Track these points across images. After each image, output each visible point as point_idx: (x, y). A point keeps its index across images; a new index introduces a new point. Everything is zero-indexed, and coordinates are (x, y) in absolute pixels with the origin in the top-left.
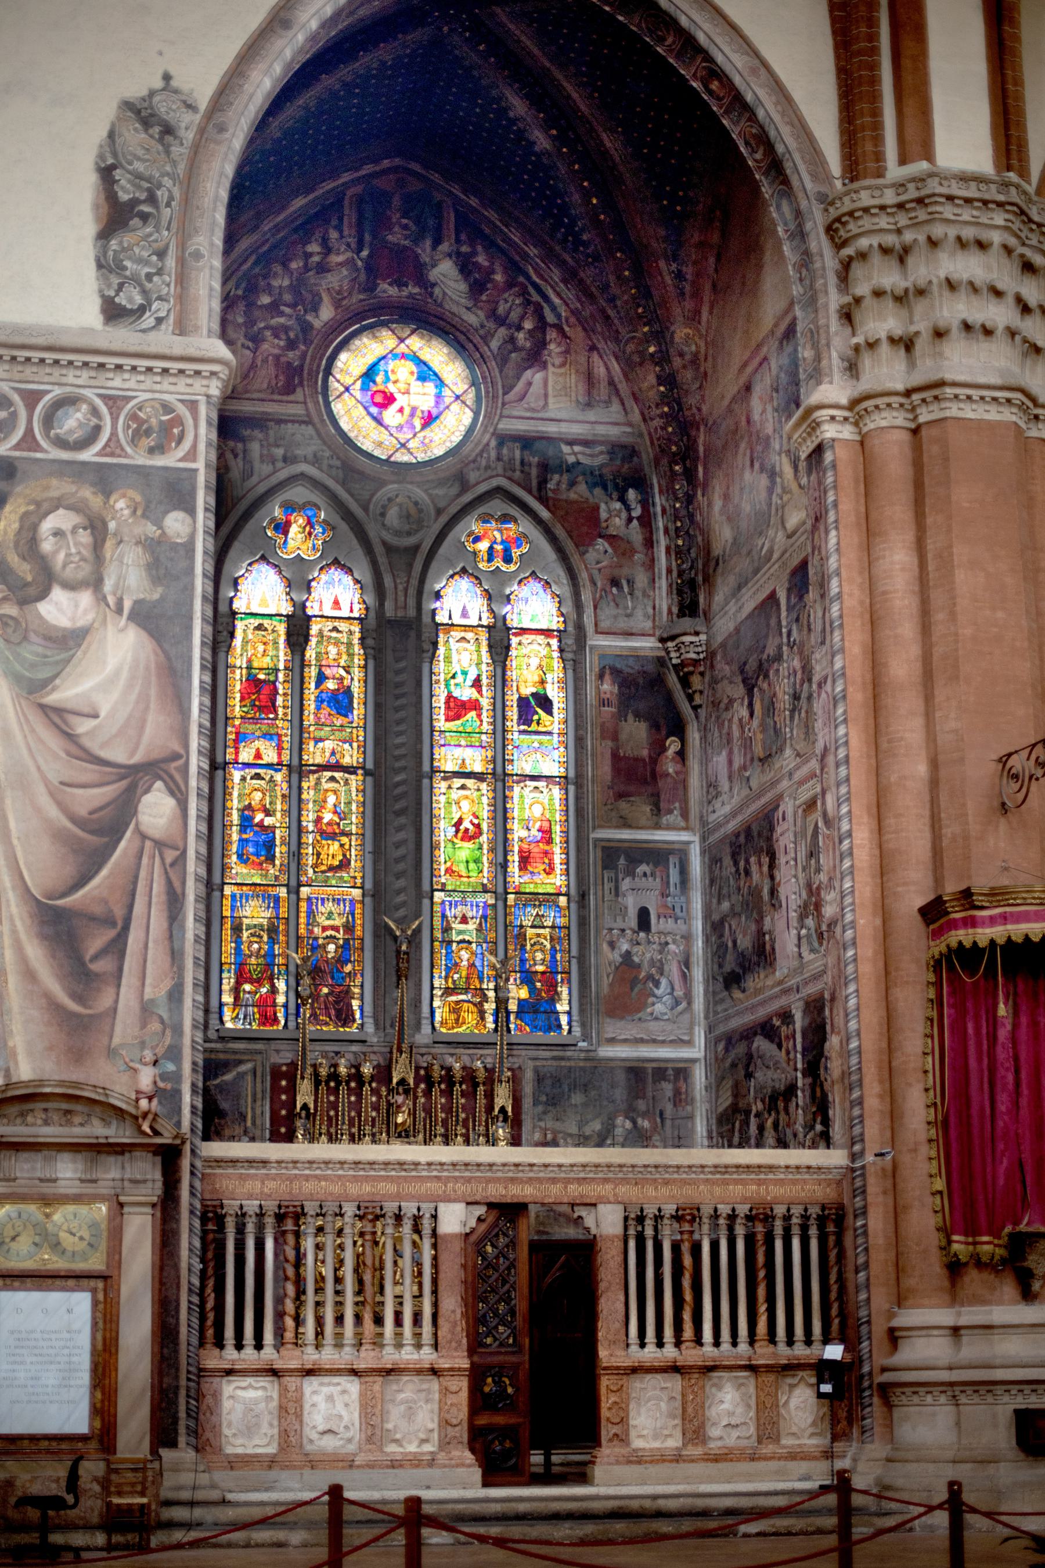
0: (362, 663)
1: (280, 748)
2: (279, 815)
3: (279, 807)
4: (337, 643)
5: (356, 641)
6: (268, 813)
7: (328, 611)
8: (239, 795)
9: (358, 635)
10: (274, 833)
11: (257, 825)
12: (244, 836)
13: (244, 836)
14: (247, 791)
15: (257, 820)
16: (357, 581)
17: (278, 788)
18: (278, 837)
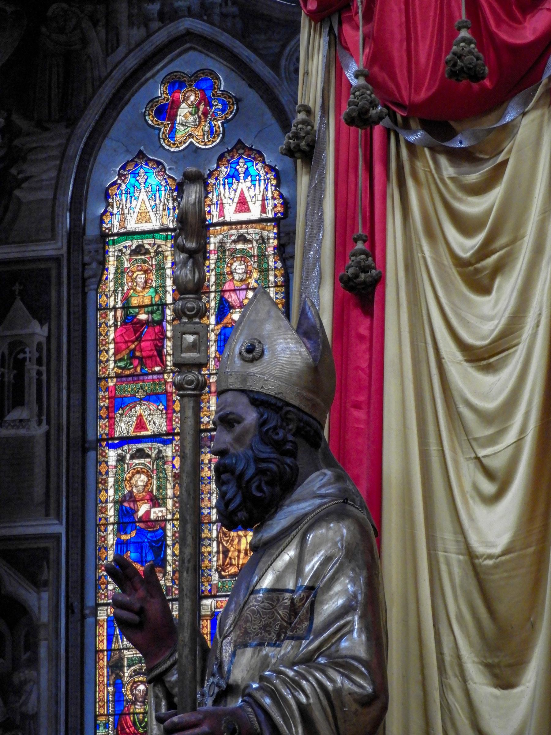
0: (280, 279)
1: (169, 410)
2: (170, 503)
3: (170, 492)
4: (245, 256)
5: (270, 251)
6: (155, 502)
7: (231, 215)
8: (116, 482)
9: (274, 242)
10: (164, 529)
11: (141, 520)
12: (124, 537)
13: (124, 537)
14: (127, 476)
15: (141, 513)
16: (272, 169)
17: (169, 467)
18: (169, 534)
